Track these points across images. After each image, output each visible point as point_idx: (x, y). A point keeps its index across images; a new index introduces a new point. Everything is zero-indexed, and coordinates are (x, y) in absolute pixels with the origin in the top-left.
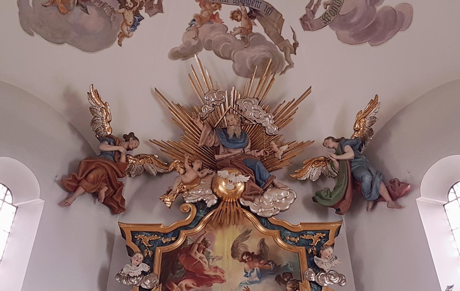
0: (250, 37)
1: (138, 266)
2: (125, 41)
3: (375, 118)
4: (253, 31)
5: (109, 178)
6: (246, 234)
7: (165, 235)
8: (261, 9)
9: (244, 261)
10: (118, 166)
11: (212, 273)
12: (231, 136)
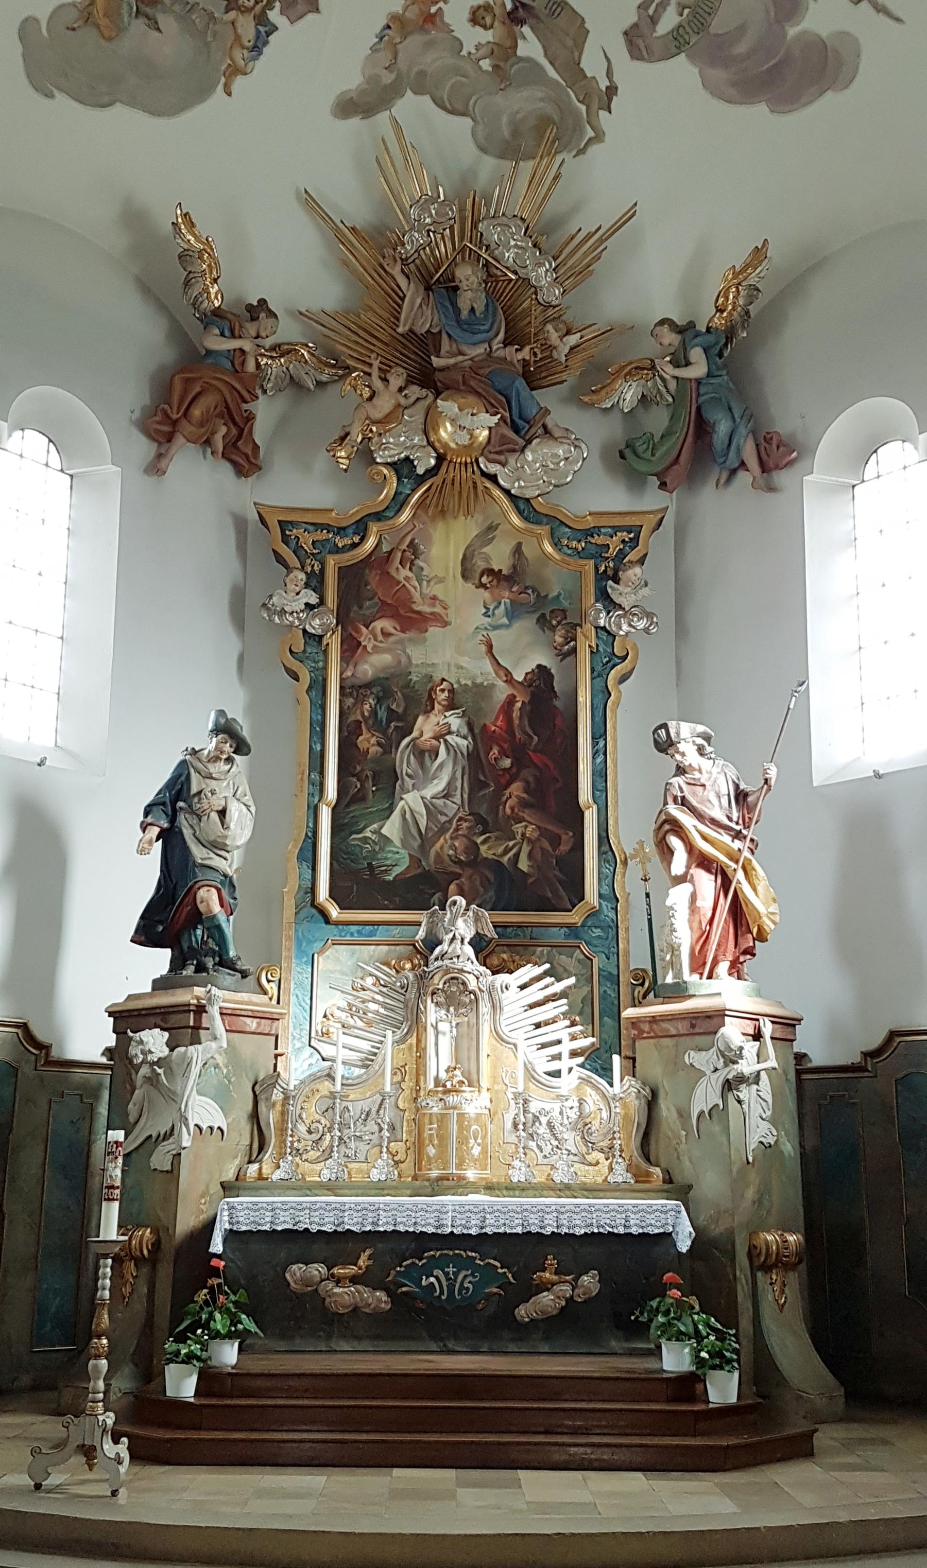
0: (512, 66)
1: (298, 594)
2: (239, 82)
3: (757, 289)
4: (519, 53)
5: (227, 408)
7: (341, 531)
9: (484, 586)
10: (241, 380)
11: (426, 609)
12: (465, 314)
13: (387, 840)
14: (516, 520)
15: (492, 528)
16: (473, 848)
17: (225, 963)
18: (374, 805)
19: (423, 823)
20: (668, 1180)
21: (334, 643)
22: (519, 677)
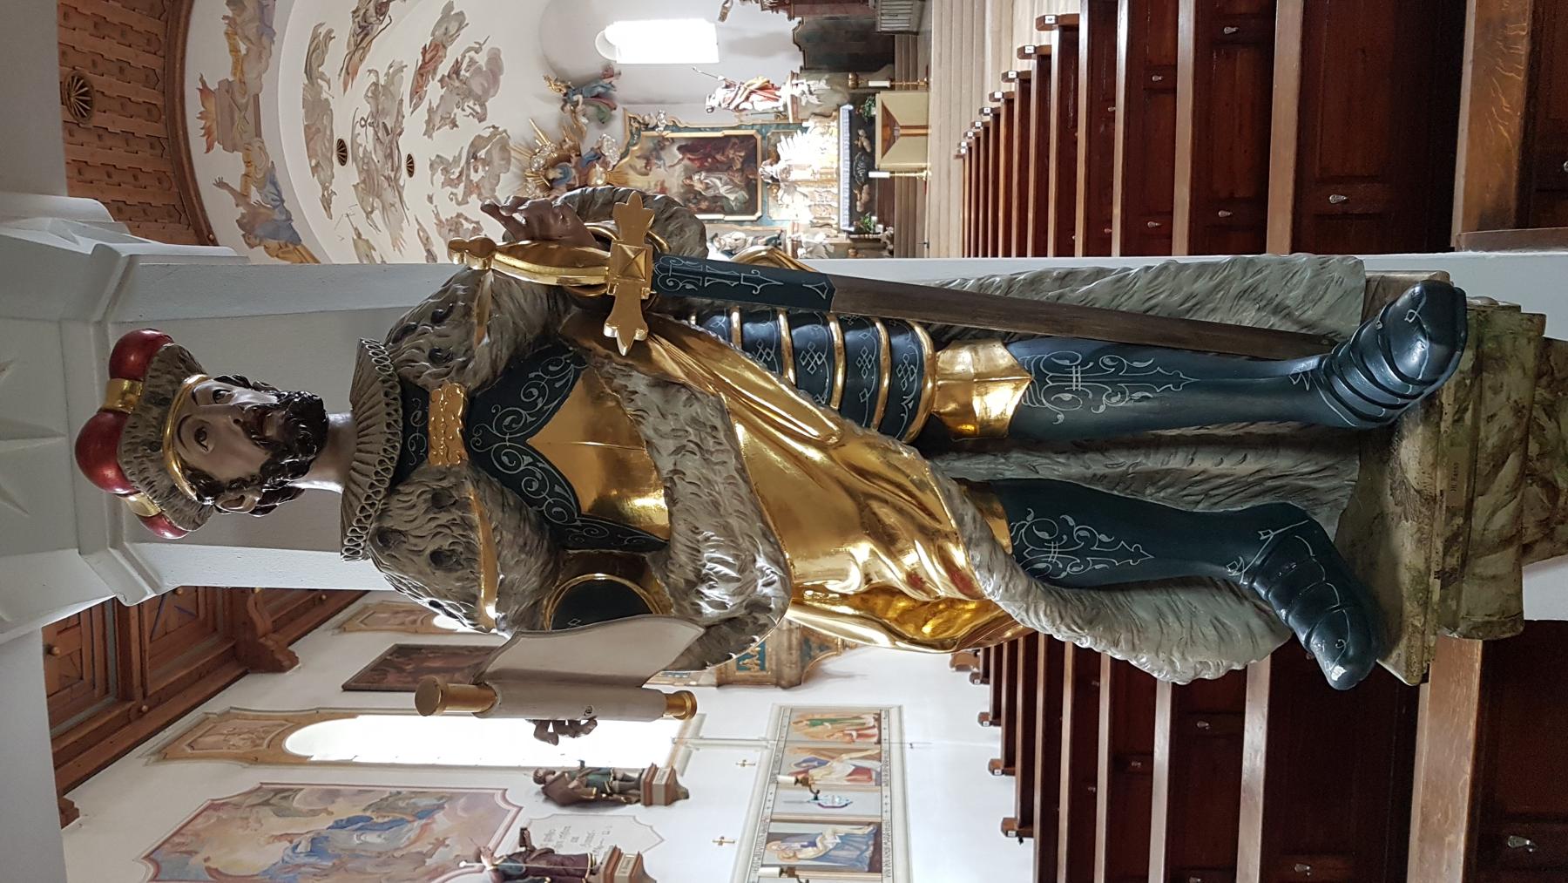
6: (632, 167)
13: (736, 198)
15: (631, 166)
16: (738, 170)
17: (778, 238)
19: (729, 187)
20: (835, 110)
22: (681, 156)
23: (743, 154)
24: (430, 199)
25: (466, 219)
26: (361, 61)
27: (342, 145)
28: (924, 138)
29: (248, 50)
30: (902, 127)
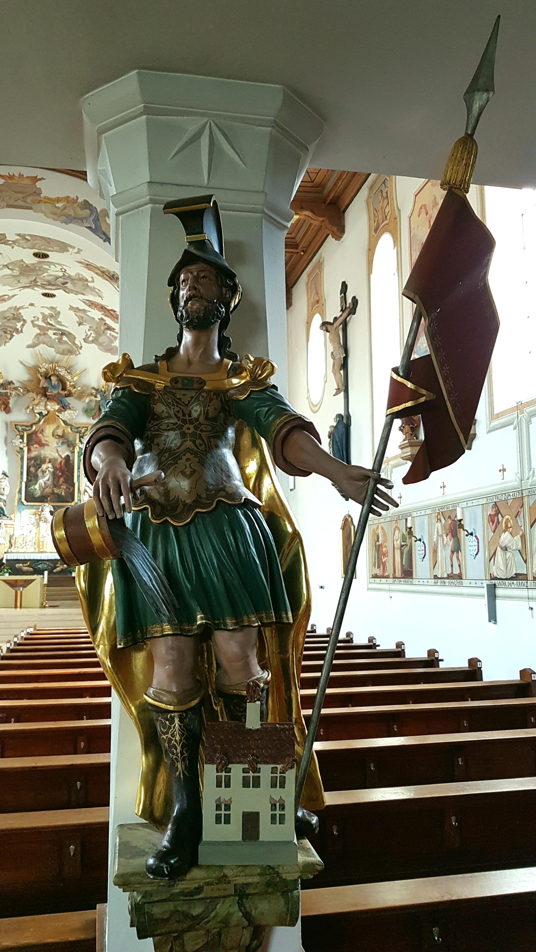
2: (7, 344)
6: (58, 427)
7: (27, 426)
8: (66, 333)
11: (44, 442)
12: (53, 384)
13: (36, 489)
14: (63, 424)
15: (58, 426)
16: (53, 491)
18: (34, 482)
21: (26, 449)
22: (63, 456)
23: (63, 494)
24: (32, 305)
25: (23, 325)
26: (97, 273)
27: (46, 256)
28: (13, 606)
29: (58, 208)
30: (21, 592)
